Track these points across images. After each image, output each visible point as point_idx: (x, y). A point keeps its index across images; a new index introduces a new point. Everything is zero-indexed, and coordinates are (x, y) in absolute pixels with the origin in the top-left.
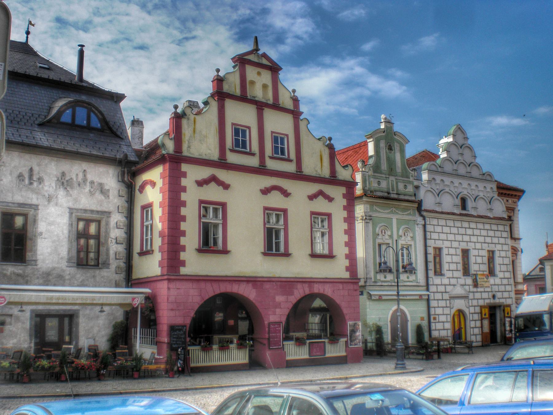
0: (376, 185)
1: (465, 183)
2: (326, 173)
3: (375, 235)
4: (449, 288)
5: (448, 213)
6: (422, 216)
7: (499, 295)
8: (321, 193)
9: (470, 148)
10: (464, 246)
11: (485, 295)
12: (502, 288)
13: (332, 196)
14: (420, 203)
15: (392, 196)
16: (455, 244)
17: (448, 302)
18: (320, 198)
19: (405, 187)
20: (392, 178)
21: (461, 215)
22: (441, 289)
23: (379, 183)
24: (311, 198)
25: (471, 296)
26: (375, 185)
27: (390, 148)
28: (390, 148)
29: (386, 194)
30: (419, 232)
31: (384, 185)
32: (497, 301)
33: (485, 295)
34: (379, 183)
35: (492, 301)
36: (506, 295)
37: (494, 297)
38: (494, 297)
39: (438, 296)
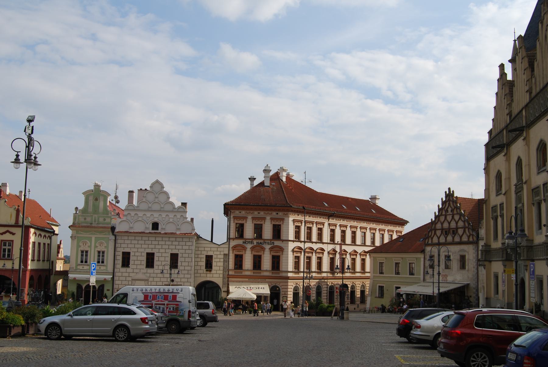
0: (83, 220)
1: (156, 215)
2: (13, 222)
3: (78, 246)
4: (131, 275)
5: (140, 233)
6: (113, 234)
8: (8, 231)
9: (166, 193)
10: (150, 251)
13: (14, 232)
14: (113, 229)
15: (93, 225)
16: (140, 250)
17: (130, 283)
18: (8, 234)
19: (105, 220)
20: (96, 216)
21: (150, 233)
22: (127, 274)
23: (85, 219)
24: (2, 234)
25: (151, 279)
26: (82, 219)
27: (96, 199)
28: (96, 199)
29: (89, 225)
30: (111, 244)
31: (89, 219)
34: (85, 219)
39: (121, 278)
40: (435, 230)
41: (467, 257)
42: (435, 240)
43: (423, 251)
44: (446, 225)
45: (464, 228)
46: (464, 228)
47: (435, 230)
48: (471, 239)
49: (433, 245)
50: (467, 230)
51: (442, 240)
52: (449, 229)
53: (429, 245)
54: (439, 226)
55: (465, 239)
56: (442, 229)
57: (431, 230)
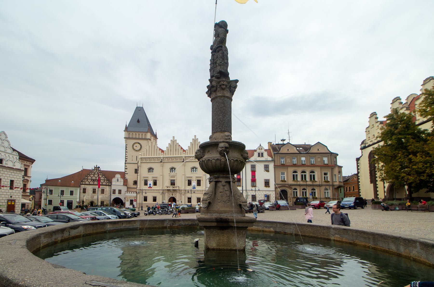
7: (13, 196)
11: (7, 196)
12: (16, 194)
32: (12, 198)
33: (7, 196)
35: (10, 198)
36: (17, 196)
37: (11, 197)
38: (11, 197)
40: (87, 179)
41: (105, 190)
42: (87, 183)
43: (80, 186)
44: (94, 178)
45: (104, 180)
46: (104, 180)
47: (87, 179)
48: (107, 184)
49: (85, 184)
50: (106, 181)
51: (91, 183)
52: (96, 180)
53: (82, 184)
54: (90, 178)
55: (104, 184)
56: (92, 179)
57: (85, 179)
